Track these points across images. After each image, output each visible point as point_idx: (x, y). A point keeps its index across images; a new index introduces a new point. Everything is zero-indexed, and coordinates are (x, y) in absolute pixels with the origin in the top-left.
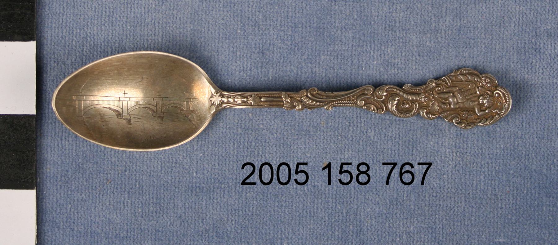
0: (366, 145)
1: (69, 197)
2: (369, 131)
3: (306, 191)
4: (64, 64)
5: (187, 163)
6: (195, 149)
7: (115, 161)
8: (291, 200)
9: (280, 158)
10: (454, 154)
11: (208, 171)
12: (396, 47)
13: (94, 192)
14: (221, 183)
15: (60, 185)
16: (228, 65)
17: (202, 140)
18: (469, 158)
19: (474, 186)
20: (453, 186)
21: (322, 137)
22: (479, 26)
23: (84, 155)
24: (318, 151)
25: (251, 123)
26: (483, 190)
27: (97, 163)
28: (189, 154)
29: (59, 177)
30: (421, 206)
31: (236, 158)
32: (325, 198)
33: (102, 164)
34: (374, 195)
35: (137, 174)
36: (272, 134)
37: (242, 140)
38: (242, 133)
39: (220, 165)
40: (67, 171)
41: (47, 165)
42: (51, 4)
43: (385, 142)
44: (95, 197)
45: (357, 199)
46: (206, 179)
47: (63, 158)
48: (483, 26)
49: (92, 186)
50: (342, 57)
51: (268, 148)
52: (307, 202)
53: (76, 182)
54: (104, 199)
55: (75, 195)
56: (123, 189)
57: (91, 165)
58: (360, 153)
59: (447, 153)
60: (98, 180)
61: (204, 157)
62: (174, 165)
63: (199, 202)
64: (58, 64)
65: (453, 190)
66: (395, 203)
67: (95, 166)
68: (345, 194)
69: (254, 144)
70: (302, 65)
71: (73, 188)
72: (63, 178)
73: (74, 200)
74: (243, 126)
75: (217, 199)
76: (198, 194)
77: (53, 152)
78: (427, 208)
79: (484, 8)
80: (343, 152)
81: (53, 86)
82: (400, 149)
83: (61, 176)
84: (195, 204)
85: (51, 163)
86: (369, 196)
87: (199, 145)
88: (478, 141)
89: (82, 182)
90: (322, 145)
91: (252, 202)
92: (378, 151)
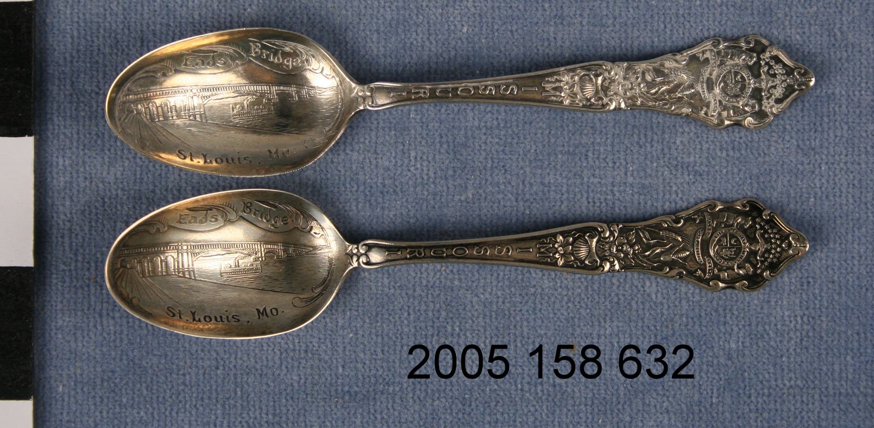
0: (643, 309)
1: (115, 418)
2: (648, 283)
3: (540, 394)
4: (103, 182)
5: (326, 352)
6: (340, 324)
7: (197, 351)
8: (512, 411)
9: (491, 338)
10: (799, 319)
11: (365, 364)
12: (692, 134)
13: (162, 406)
14: (387, 383)
15: (101, 397)
16: (395, 174)
17: (350, 310)
18: (824, 326)
19: (836, 375)
20: (798, 375)
21: (566, 298)
22: (837, 91)
23: (143, 343)
24: (558, 323)
25: (438, 276)
26: (851, 381)
27: (166, 356)
28: (331, 335)
29: (99, 382)
30: (743, 414)
31: (413, 339)
32: (574, 406)
33: (175, 357)
34: (659, 398)
35: (239, 372)
36: (477, 295)
37: (423, 307)
38: (423, 294)
39: (386, 353)
40: (112, 371)
41: (76, 362)
42: (76, 75)
43: (677, 303)
44: (163, 416)
45: (630, 405)
46: (360, 376)
47: (104, 349)
48: (843, 93)
49: (158, 397)
50: (596, 156)
51: (470, 321)
52: (541, 414)
53: (128, 391)
54: (180, 418)
55: (127, 414)
56: (214, 401)
57: (155, 360)
58: (633, 324)
59: (786, 318)
60: (167, 385)
61: (357, 339)
62: (303, 356)
63: (350, 418)
64: (91, 182)
65: (799, 382)
66: (696, 408)
67: (163, 361)
68: (608, 398)
69: (444, 313)
70: (525, 172)
71: (124, 400)
72: (105, 384)
73: (126, 422)
74: (424, 282)
75: (381, 413)
76: (345, 405)
77: (87, 339)
78: (752, 415)
79: (843, 61)
80: (603, 324)
81: (84, 221)
82: (703, 314)
83: (102, 380)
84: (343, 422)
85: (84, 357)
86: (651, 399)
87: (347, 317)
88: (839, 294)
89: (139, 390)
90: (566, 314)
91: (443, 416)
92: (663, 319)
